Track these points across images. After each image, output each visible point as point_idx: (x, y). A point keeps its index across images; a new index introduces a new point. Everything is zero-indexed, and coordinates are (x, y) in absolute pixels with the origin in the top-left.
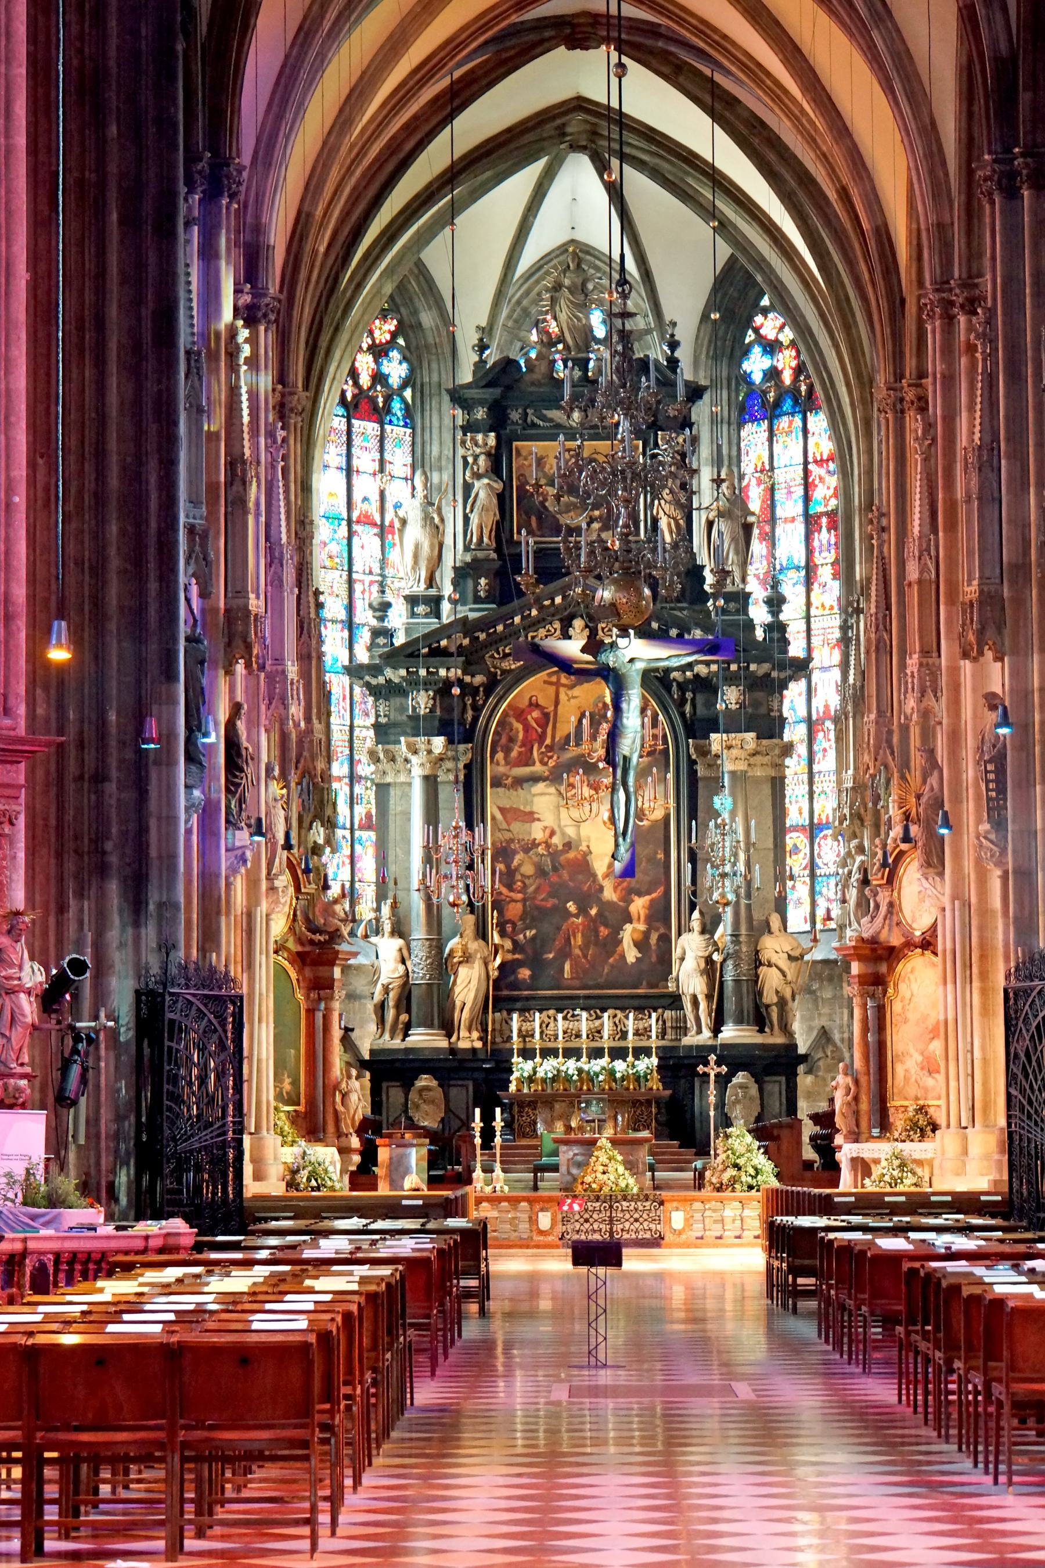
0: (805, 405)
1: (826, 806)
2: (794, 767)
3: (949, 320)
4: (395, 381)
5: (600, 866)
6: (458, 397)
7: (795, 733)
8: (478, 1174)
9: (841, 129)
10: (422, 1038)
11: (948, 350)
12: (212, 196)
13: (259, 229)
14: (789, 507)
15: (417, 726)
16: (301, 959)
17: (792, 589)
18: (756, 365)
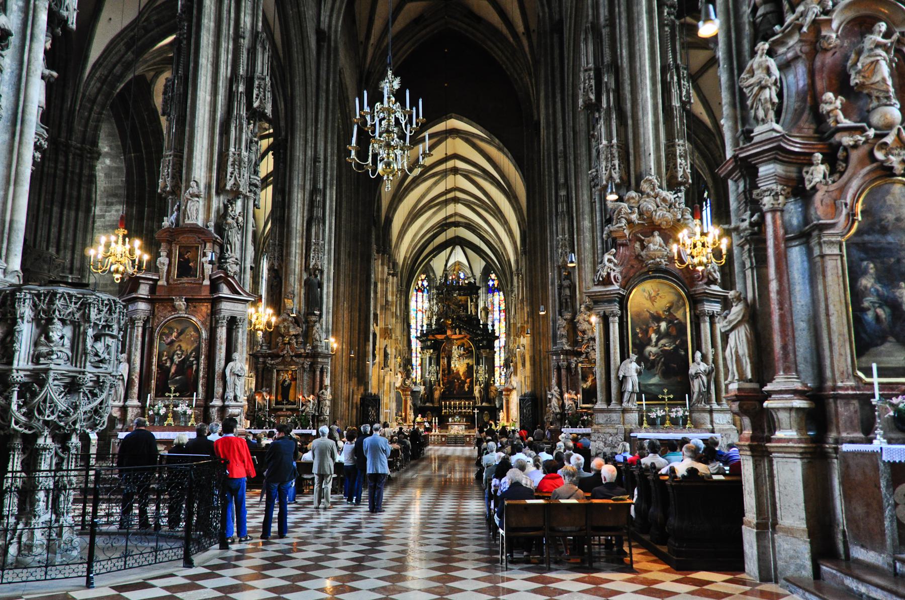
0: (499, 291)
1: (502, 363)
2: (497, 356)
3: (518, 276)
4: (425, 285)
5: (461, 373)
6: (437, 288)
7: (497, 349)
8: (433, 430)
9: (501, 242)
10: (427, 404)
11: (518, 282)
12: (383, 255)
13: (395, 260)
14: (496, 309)
15: (429, 348)
16: (403, 391)
17: (497, 323)
18: (491, 283)
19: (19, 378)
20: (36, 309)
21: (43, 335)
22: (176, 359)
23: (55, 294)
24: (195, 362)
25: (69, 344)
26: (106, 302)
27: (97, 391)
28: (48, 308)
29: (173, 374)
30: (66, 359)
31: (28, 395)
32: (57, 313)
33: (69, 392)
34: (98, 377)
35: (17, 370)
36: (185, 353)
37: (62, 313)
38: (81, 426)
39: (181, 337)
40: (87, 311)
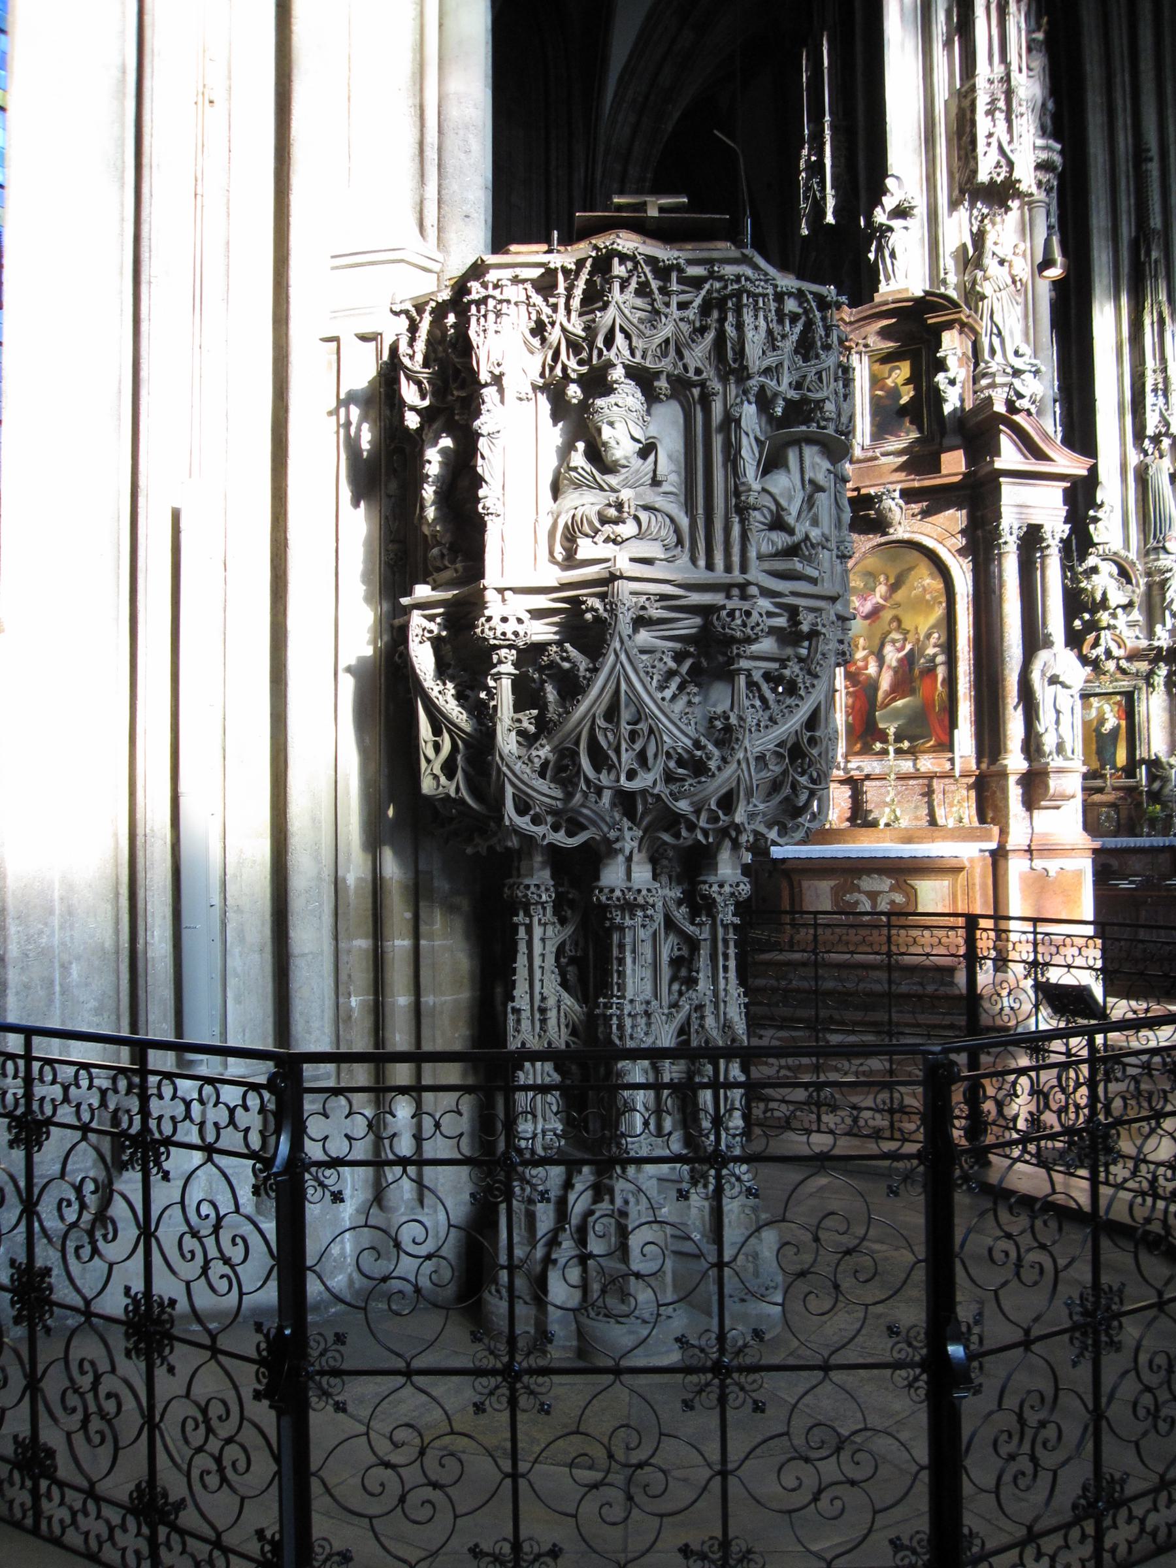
19: (512, 620)
20: (543, 340)
21: (581, 446)
22: (892, 655)
23: (602, 264)
24: (940, 659)
25: (673, 478)
26: (791, 305)
27: (793, 670)
28: (587, 328)
29: (887, 694)
30: (673, 539)
31: (551, 693)
32: (619, 338)
33: (696, 675)
34: (793, 612)
35: (501, 591)
36: (911, 637)
37: (638, 343)
38: (751, 816)
39: (899, 595)
40: (730, 331)
